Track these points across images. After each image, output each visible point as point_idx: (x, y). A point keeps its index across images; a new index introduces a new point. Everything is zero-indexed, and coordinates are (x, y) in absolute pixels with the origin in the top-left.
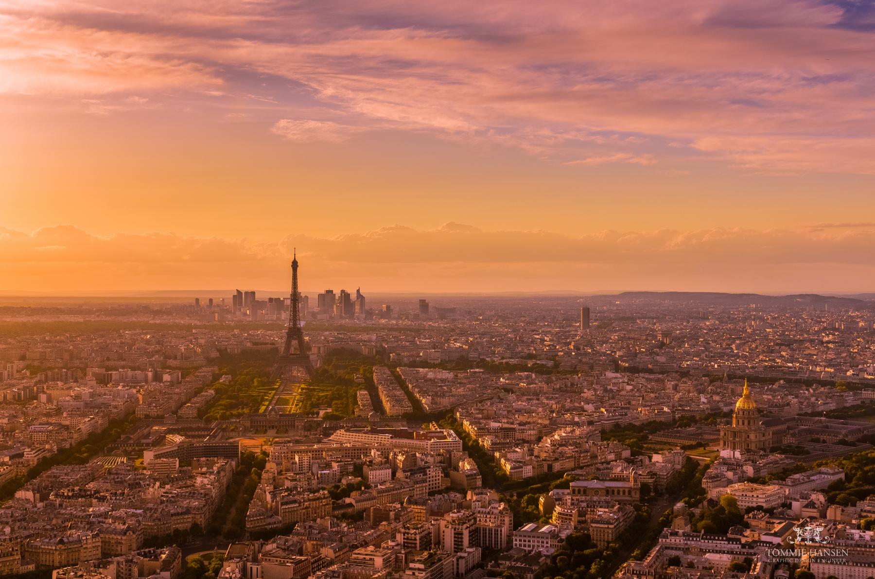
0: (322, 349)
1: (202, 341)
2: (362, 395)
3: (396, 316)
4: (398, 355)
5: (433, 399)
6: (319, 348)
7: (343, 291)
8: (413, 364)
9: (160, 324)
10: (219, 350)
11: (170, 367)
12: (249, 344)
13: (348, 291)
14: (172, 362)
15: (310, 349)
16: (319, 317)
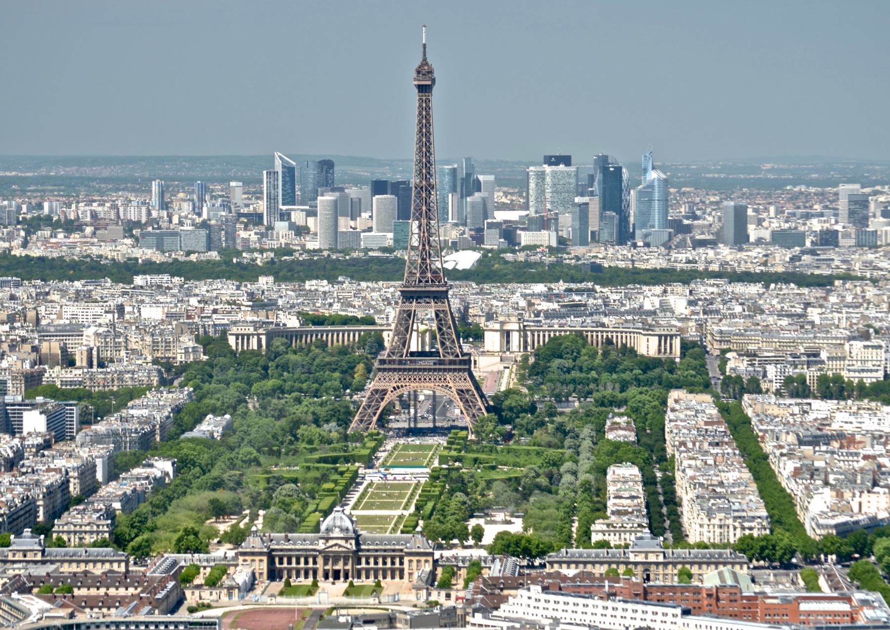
0: (515, 337)
1: (152, 313)
2: (624, 481)
3: (767, 235)
4: (752, 355)
5: (840, 495)
6: (508, 334)
7: (603, 162)
8: (797, 389)
9: (42, 259)
10: (205, 342)
11: (53, 392)
12: (293, 323)
13: (618, 157)
14: (56, 375)
15: (478, 336)
16: (525, 238)
